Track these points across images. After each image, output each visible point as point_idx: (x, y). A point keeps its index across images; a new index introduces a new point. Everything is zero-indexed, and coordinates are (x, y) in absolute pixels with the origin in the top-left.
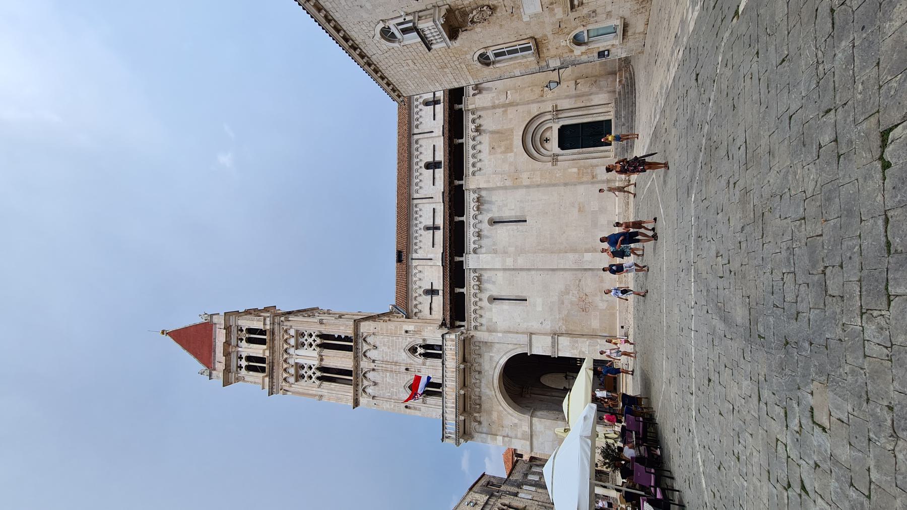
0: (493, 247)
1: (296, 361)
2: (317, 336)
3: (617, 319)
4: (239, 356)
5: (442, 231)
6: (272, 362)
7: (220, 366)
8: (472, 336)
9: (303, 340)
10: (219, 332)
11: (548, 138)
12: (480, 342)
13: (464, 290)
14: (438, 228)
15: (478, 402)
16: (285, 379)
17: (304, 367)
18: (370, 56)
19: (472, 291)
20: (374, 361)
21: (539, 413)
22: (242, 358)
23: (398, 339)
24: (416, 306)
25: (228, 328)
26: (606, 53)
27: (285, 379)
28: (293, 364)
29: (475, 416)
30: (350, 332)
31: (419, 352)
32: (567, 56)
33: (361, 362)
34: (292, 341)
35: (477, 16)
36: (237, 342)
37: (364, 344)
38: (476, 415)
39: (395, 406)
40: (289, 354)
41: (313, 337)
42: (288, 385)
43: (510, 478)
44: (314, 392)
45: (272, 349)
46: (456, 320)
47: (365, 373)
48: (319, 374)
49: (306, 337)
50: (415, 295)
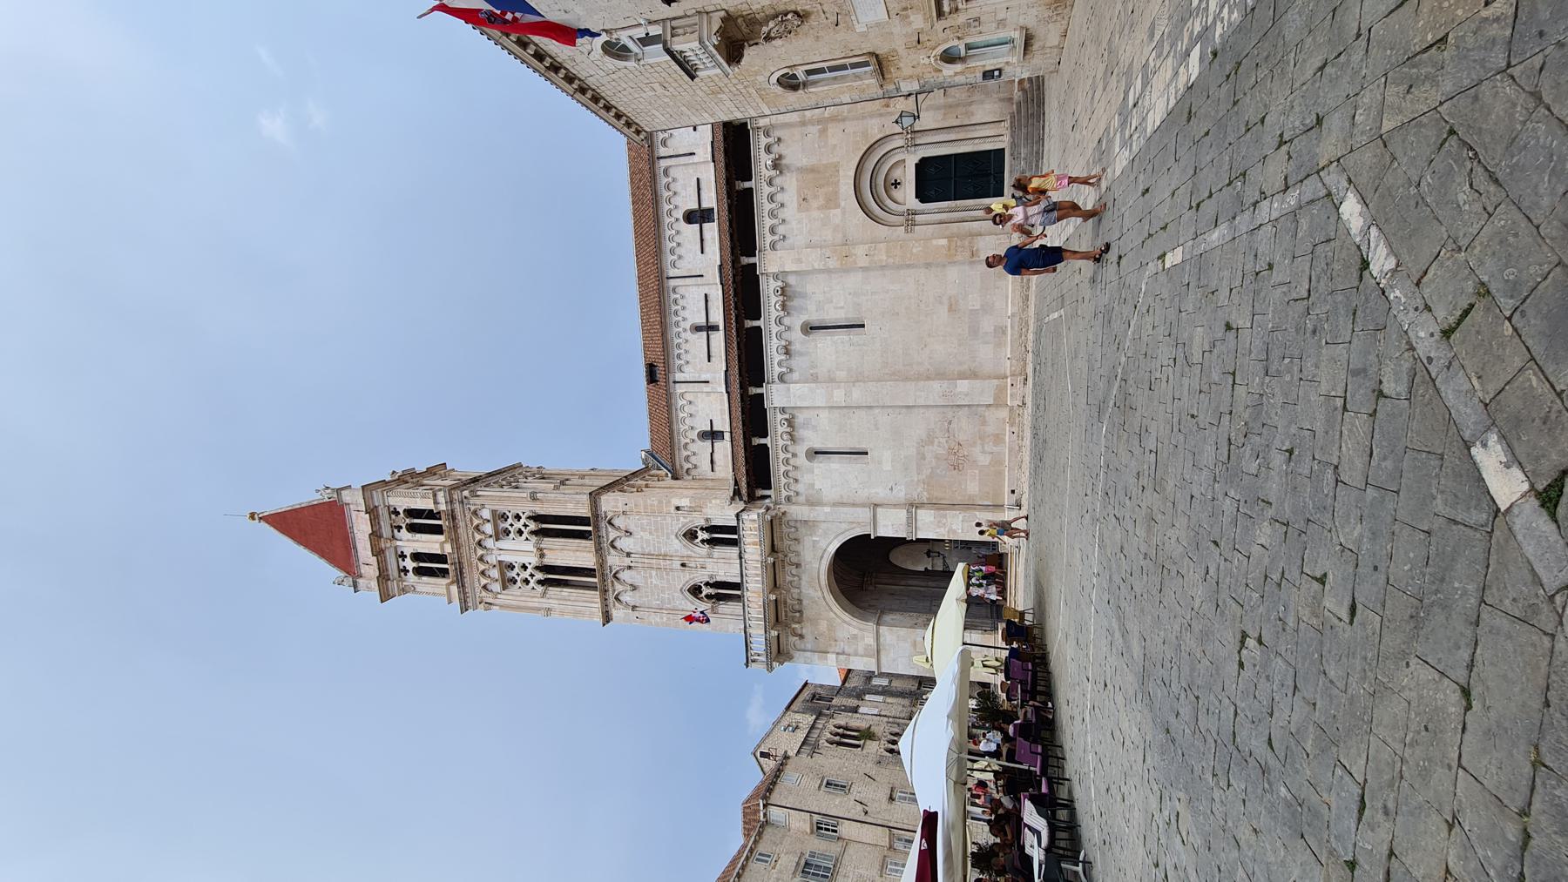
0: (811, 371)
1: (499, 558)
2: (529, 518)
3: (1005, 480)
4: (399, 553)
5: (722, 332)
6: (459, 563)
7: (370, 570)
8: (784, 514)
9: (506, 525)
10: (357, 516)
11: (898, 181)
12: (796, 521)
13: (767, 441)
14: (715, 328)
15: (797, 607)
16: (485, 587)
17: (514, 567)
18: (583, 78)
19: (781, 443)
20: (628, 555)
21: (888, 618)
22: (406, 556)
23: (665, 520)
24: (687, 459)
25: (372, 511)
26: (996, 73)
27: (485, 587)
28: (495, 563)
29: (793, 629)
30: (584, 511)
31: (700, 538)
32: (931, 78)
33: (608, 557)
34: (489, 529)
35: (777, 28)
36: (393, 531)
37: (610, 529)
38: (794, 626)
39: (668, 619)
40: (485, 548)
41: (523, 520)
42: (490, 595)
43: (846, 685)
44: (536, 605)
45: (456, 542)
46: (757, 487)
48: (540, 576)
49: (510, 521)
50: (683, 441)
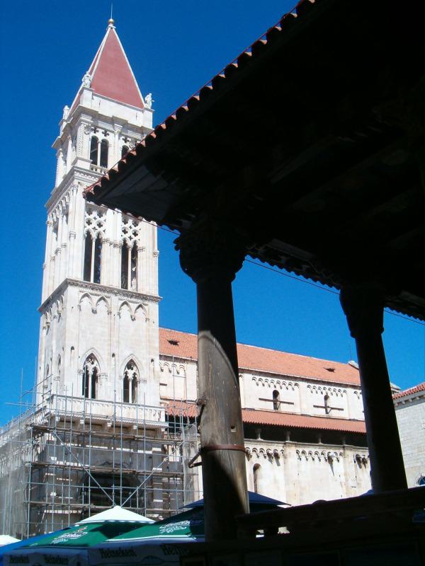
2: (135, 243)
20: (119, 314)
47: (104, 299)
49: (134, 228)
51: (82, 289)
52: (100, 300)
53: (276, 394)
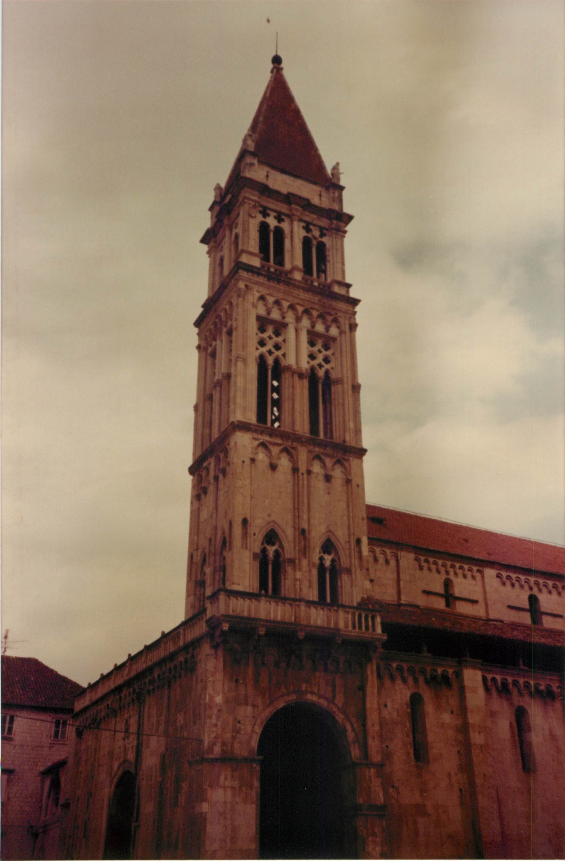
2: (327, 372)
4: (283, 217)
34: (320, 328)
48: (270, 360)
49: (324, 353)
51: (256, 436)
52: (282, 451)
53: (533, 600)
